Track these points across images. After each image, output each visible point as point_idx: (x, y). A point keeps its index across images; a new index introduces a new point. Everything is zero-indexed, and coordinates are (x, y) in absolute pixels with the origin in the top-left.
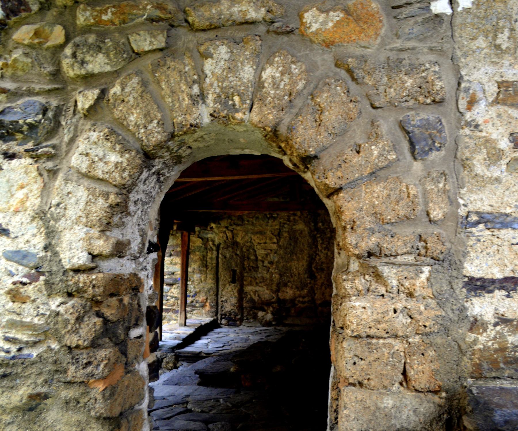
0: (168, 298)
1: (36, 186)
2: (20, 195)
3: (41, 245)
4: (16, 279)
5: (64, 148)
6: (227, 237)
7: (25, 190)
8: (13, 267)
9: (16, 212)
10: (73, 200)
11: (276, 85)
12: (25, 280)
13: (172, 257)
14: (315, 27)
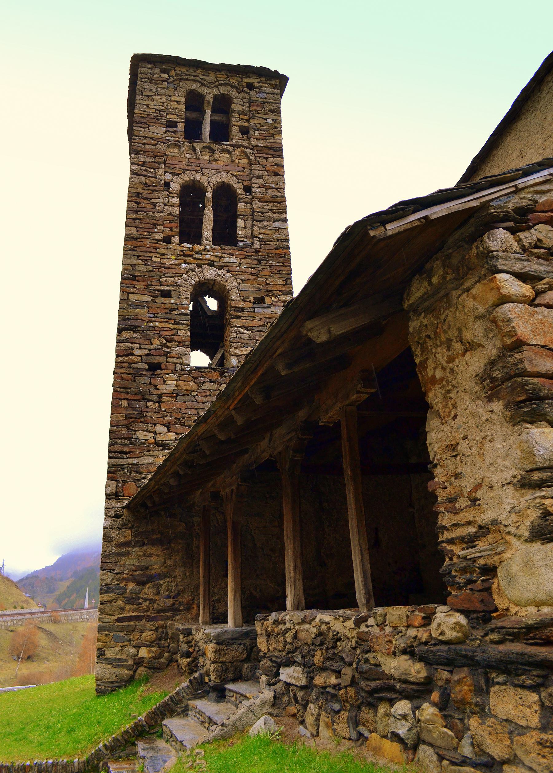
0: (140, 601)
6: (217, 521)
13: (145, 548)
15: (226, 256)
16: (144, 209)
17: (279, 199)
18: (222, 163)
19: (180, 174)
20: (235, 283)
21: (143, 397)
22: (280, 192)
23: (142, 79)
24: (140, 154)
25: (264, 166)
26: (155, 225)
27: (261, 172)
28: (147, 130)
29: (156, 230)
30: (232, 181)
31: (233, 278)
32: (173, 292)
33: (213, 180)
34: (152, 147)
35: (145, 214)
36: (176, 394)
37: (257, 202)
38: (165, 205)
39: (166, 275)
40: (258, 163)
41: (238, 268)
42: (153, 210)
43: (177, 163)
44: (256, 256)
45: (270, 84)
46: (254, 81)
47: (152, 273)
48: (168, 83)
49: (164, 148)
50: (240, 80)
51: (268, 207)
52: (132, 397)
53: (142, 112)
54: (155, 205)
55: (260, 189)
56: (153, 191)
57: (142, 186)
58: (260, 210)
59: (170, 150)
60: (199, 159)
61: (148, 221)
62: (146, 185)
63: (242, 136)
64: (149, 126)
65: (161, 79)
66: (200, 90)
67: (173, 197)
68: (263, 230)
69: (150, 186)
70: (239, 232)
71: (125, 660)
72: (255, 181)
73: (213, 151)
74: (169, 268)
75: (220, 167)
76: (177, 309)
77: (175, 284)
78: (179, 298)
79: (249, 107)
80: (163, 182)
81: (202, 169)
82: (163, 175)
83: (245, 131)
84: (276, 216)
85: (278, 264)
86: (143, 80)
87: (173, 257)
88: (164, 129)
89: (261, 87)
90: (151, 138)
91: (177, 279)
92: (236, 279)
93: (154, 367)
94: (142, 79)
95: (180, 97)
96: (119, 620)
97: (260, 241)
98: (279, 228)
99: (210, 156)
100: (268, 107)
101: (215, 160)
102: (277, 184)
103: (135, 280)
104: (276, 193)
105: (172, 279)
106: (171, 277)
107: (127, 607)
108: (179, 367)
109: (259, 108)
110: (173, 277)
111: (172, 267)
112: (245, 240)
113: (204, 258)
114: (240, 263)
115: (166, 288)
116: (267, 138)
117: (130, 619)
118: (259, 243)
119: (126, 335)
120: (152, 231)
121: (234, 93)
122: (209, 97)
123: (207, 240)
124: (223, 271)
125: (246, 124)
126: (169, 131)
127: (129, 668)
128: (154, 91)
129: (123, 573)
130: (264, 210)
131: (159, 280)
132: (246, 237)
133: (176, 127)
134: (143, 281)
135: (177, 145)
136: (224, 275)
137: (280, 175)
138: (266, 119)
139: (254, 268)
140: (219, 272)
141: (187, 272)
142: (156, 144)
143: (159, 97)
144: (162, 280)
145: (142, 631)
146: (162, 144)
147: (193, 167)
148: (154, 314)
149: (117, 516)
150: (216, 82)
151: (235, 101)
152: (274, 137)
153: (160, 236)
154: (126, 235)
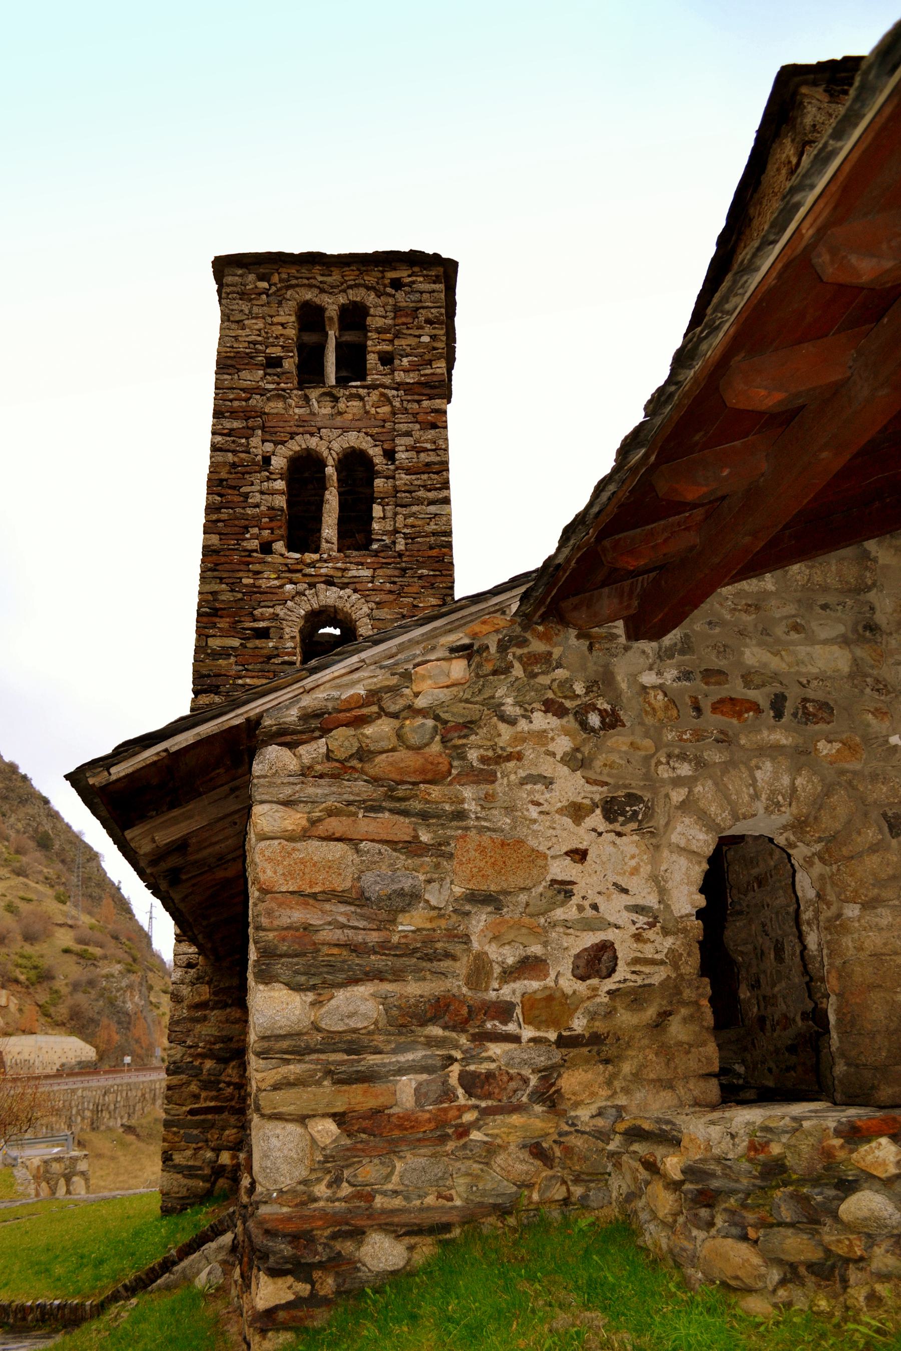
0: (221, 1086)
1: (645, 857)
2: (633, 863)
3: (656, 900)
4: (638, 925)
5: (662, 829)
7: (636, 860)
8: (634, 916)
9: (632, 874)
10: (677, 867)
11: (804, 790)
12: (645, 926)
13: (228, 1010)
14: (825, 752)
15: (353, 567)
16: (231, 505)
17: (436, 468)
18: (350, 416)
19: (286, 442)
20: (365, 609)
22: (438, 455)
23: (228, 294)
24: (225, 417)
25: (415, 415)
26: (246, 529)
27: (410, 425)
28: (236, 377)
29: (248, 536)
30: (365, 443)
31: (363, 600)
32: (272, 630)
33: (336, 446)
34: (244, 403)
35: (231, 511)
37: (403, 476)
38: (262, 493)
39: (262, 604)
40: (406, 411)
41: (370, 585)
42: (243, 505)
43: (281, 424)
44: (399, 563)
45: (427, 276)
46: (402, 274)
47: (241, 604)
48: (268, 296)
49: (260, 404)
50: (380, 275)
51: (419, 482)
53: (228, 350)
55: (407, 454)
56: (243, 474)
57: (228, 468)
58: (407, 488)
59: (272, 404)
60: (314, 414)
61: (236, 522)
62: (234, 465)
63: (381, 368)
64: (239, 370)
65: (257, 291)
66: (317, 301)
67: (275, 480)
68: (410, 521)
69: (239, 466)
70: (375, 526)
71: (200, 1168)
73: (336, 399)
74: (266, 593)
75: (347, 424)
76: (278, 656)
77: (275, 618)
78: (281, 638)
79: (394, 318)
80: (259, 458)
81: (319, 429)
82: (258, 446)
83: (386, 359)
84: (432, 495)
85: (432, 573)
86: (230, 296)
87: (273, 576)
88: (261, 372)
89: (414, 282)
90: (241, 390)
91: (279, 610)
92: (367, 602)
94: (228, 294)
95: (287, 316)
96: (192, 1112)
97: (405, 538)
98: (436, 515)
99: (333, 407)
100: (423, 315)
101: (340, 413)
102: (435, 443)
103: (216, 616)
104: (433, 458)
105: (271, 610)
106: (269, 607)
107: (203, 1094)
109: (409, 320)
110: (272, 607)
111: (271, 591)
112: (384, 538)
113: (318, 573)
114: (373, 577)
115: (262, 624)
116: (421, 368)
117: (207, 1110)
118: (403, 542)
120: (241, 537)
121: (371, 299)
122: (332, 311)
123: (327, 542)
124: (347, 590)
125: (388, 348)
126: (270, 375)
127: (204, 1179)
128: (247, 312)
129: (197, 1046)
130: (412, 488)
131: (252, 613)
132: (385, 533)
133: (281, 366)
134: (228, 616)
135: (281, 396)
136: (349, 597)
137: (439, 427)
138: (419, 336)
139: (394, 583)
140: (342, 592)
141: (293, 597)
142: (249, 399)
143: (254, 321)
144: (256, 612)
145: (223, 1129)
146: (258, 397)
147: (306, 429)
148: (243, 665)
149: (190, 965)
150: (342, 284)
151: (372, 311)
152: (431, 365)
153: (254, 544)
154: (205, 547)
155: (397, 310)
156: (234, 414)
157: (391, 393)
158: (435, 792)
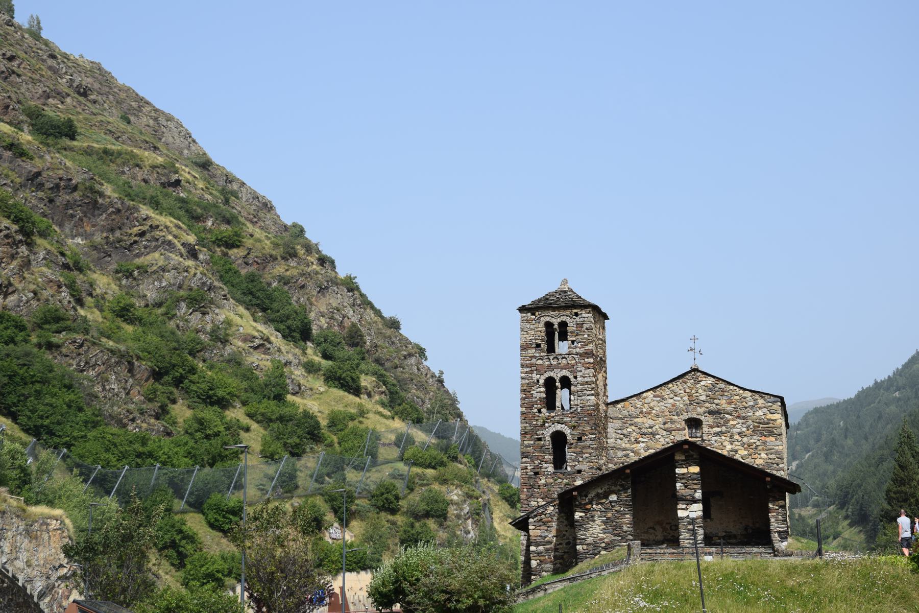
17: (590, 383)
18: (562, 365)
20: (569, 431)
21: (532, 487)
33: (559, 375)
36: (545, 485)
52: (528, 487)
54: (532, 394)
62: (528, 384)
68: (582, 402)
72: (579, 374)
79: (577, 327)
80: (536, 381)
83: (573, 342)
91: (544, 432)
93: (536, 474)
95: (541, 327)
100: (585, 326)
108: (546, 473)
115: (539, 437)
119: (524, 460)
121: (568, 320)
122: (556, 326)
124: (563, 426)
125: (574, 339)
151: (569, 325)
153: (536, 410)
155: (577, 324)
156: (527, 366)
157: (576, 356)
158: (550, 524)
